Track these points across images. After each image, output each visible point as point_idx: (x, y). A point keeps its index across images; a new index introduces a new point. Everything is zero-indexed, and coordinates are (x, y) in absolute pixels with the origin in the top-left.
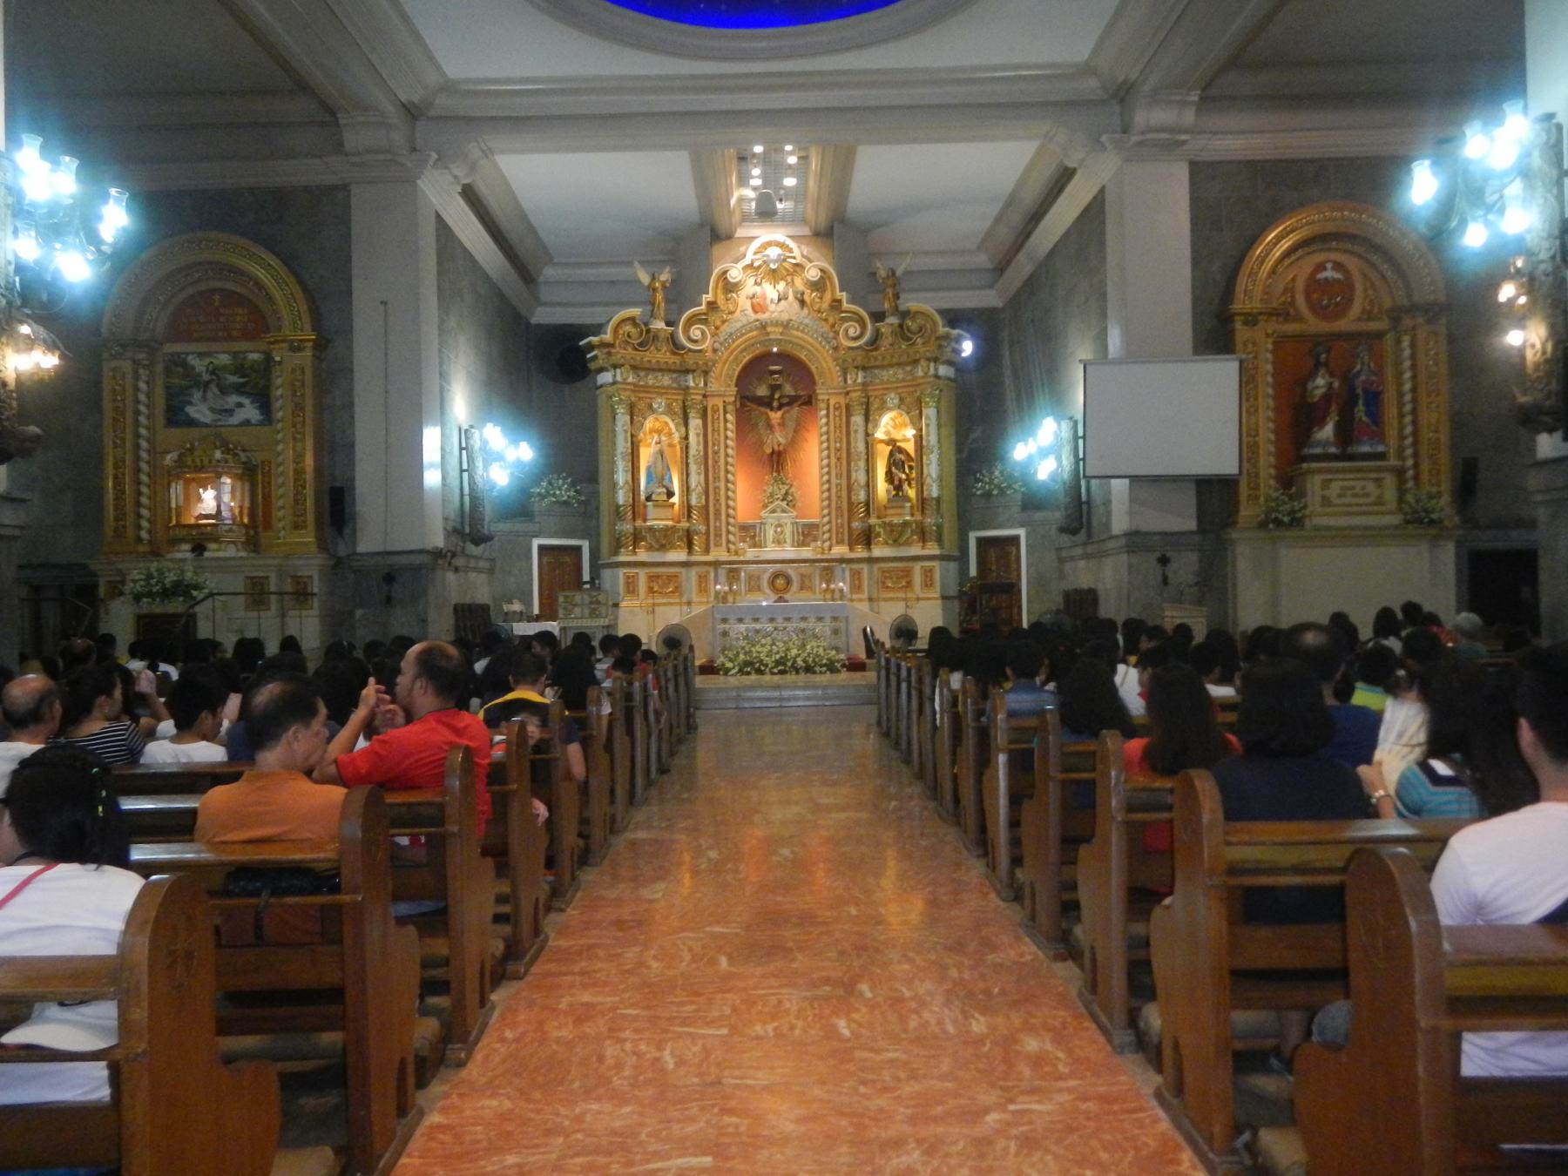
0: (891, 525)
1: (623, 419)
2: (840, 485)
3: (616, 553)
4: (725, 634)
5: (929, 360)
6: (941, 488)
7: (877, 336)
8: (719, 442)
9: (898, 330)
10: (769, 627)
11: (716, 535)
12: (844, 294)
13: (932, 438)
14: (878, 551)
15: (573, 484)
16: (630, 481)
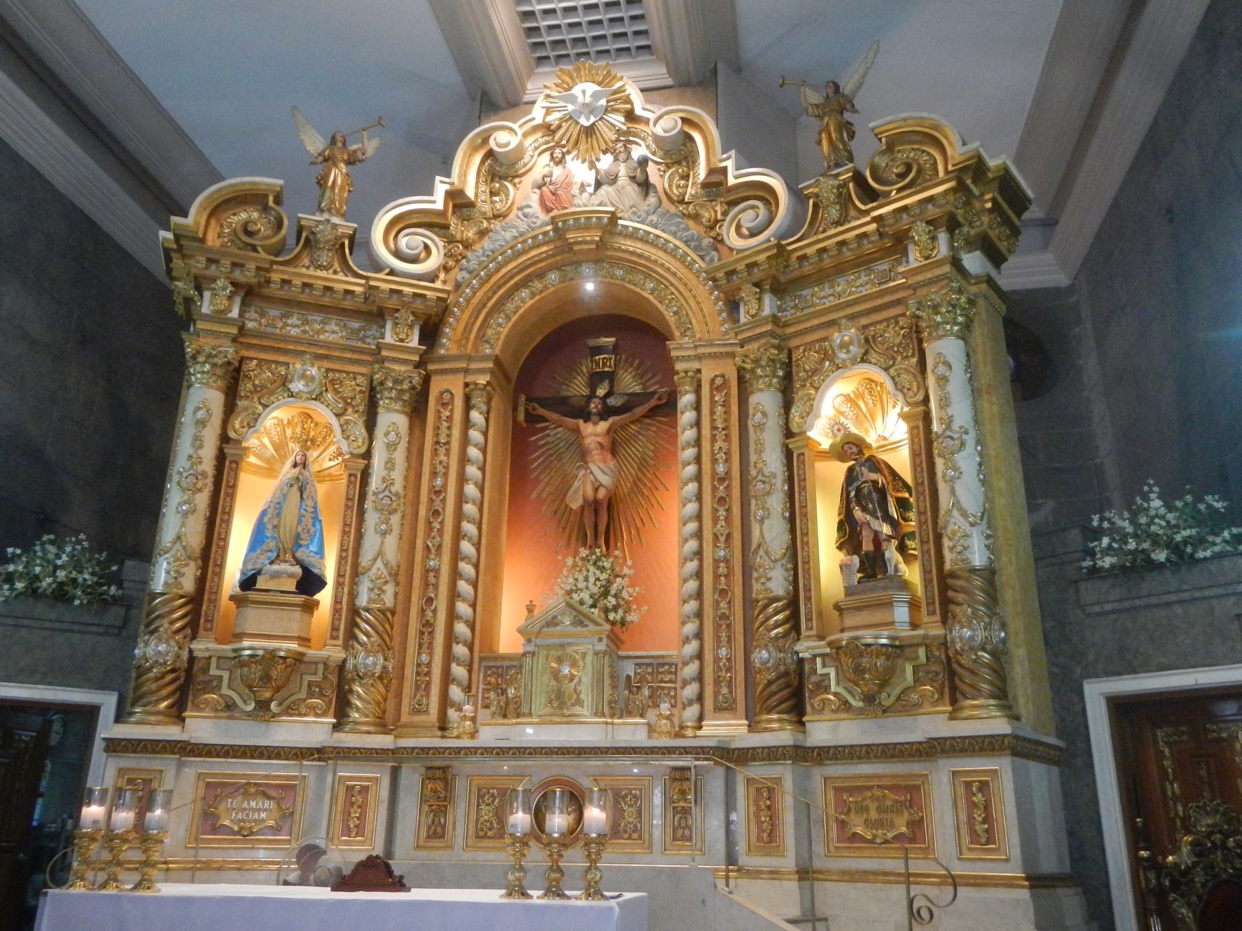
2: (727, 561)
5: (929, 223)
8: (447, 468)
9: (851, 185)
11: (417, 687)
12: (733, 153)
16: (195, 540)
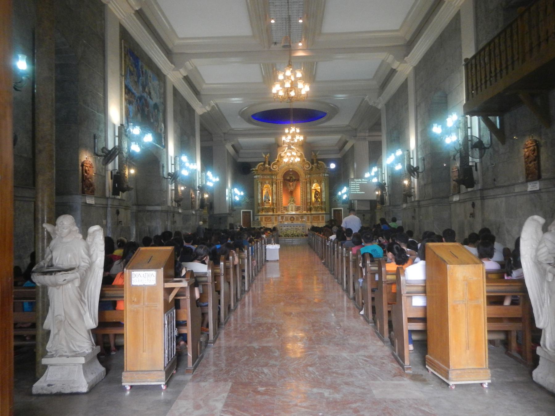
0: (315, 207)
1: (260, 185)
3: (258, 213)
4: (281, 229)
5: (323, 173)
6: (325, 200)
7: (312, 168)
10: (290, 228)
13: (324, 189)
14: (313, 212)
15: (249, 199)
